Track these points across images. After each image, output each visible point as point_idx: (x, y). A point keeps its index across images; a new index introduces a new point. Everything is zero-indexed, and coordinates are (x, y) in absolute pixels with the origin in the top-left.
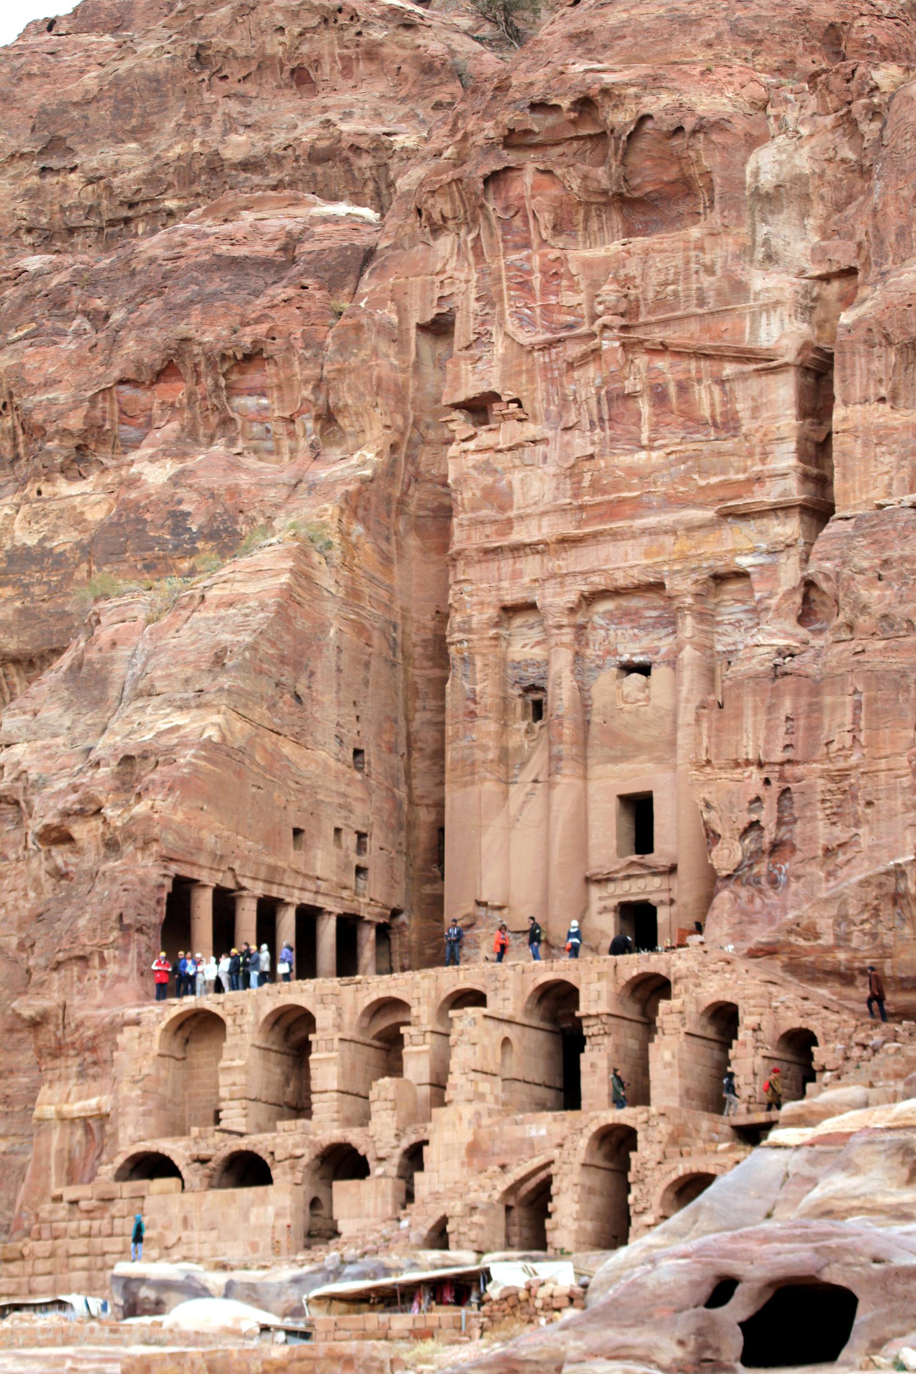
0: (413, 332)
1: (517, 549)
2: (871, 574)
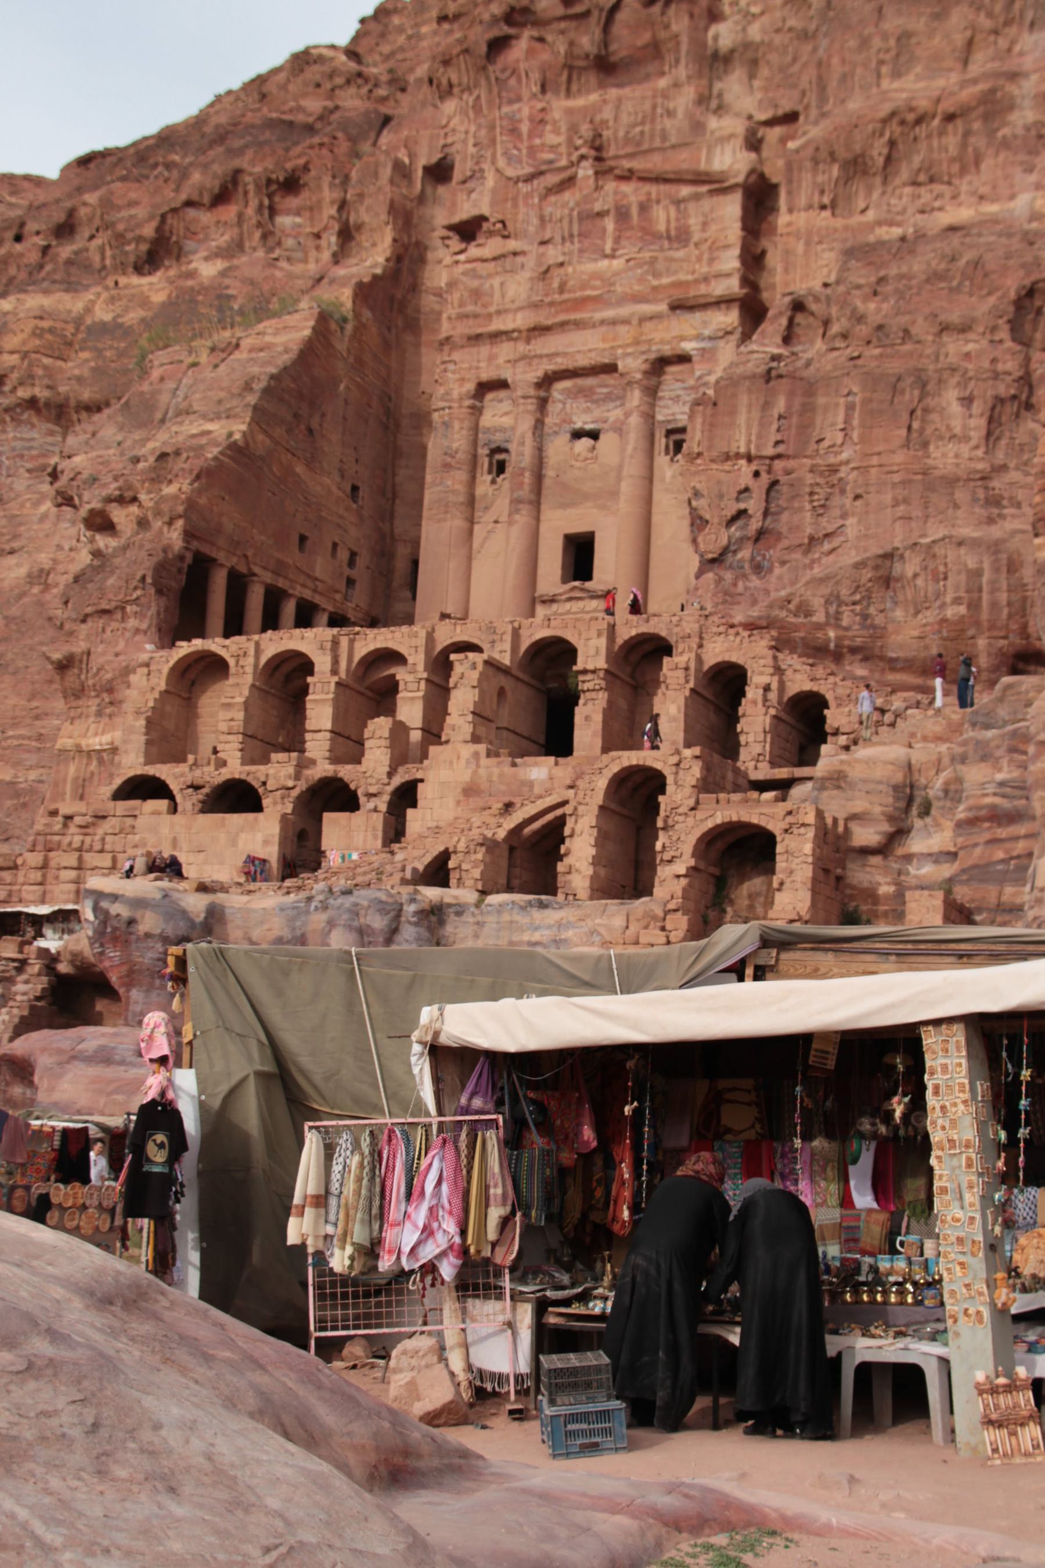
0: (420, 173)
1: (496, 336)
2: (867, 290)
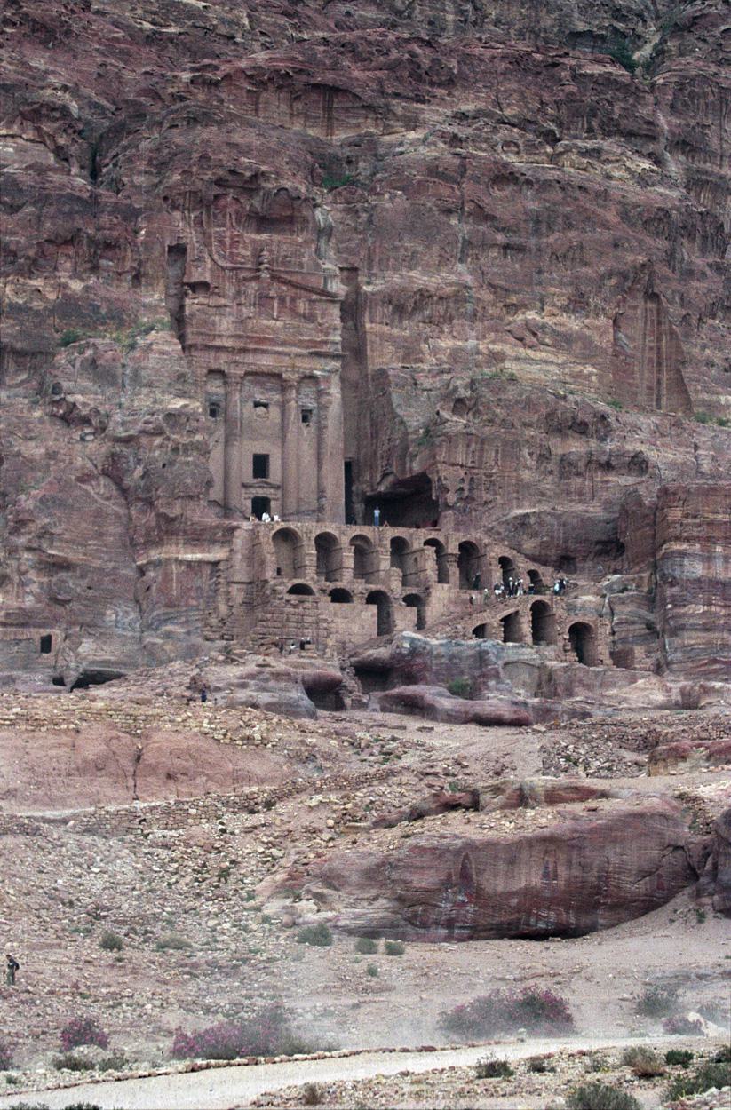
1: (219, 349)
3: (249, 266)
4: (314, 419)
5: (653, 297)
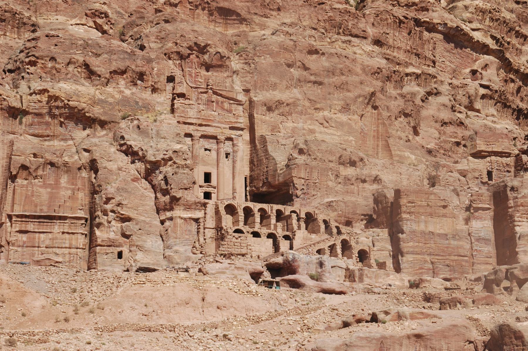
3: (203, 87)
4: (231, 157)
5: (375, 108)
